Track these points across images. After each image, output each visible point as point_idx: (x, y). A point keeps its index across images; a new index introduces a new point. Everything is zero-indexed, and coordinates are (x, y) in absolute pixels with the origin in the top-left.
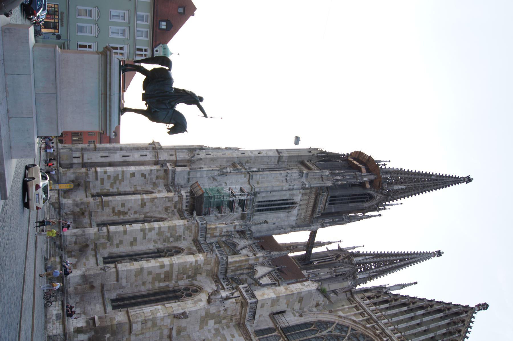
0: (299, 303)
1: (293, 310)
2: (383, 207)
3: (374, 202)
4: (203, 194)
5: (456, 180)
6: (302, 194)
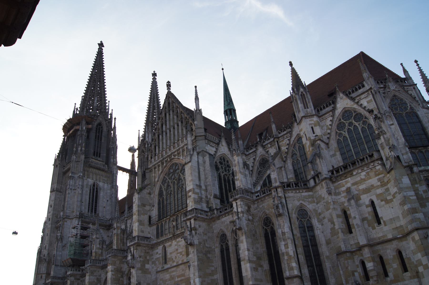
0: (145, 206)
2: (109, 115)
3: (104, 123)
4: (71, 259)
5: (100, 55)
6: (88, 178)
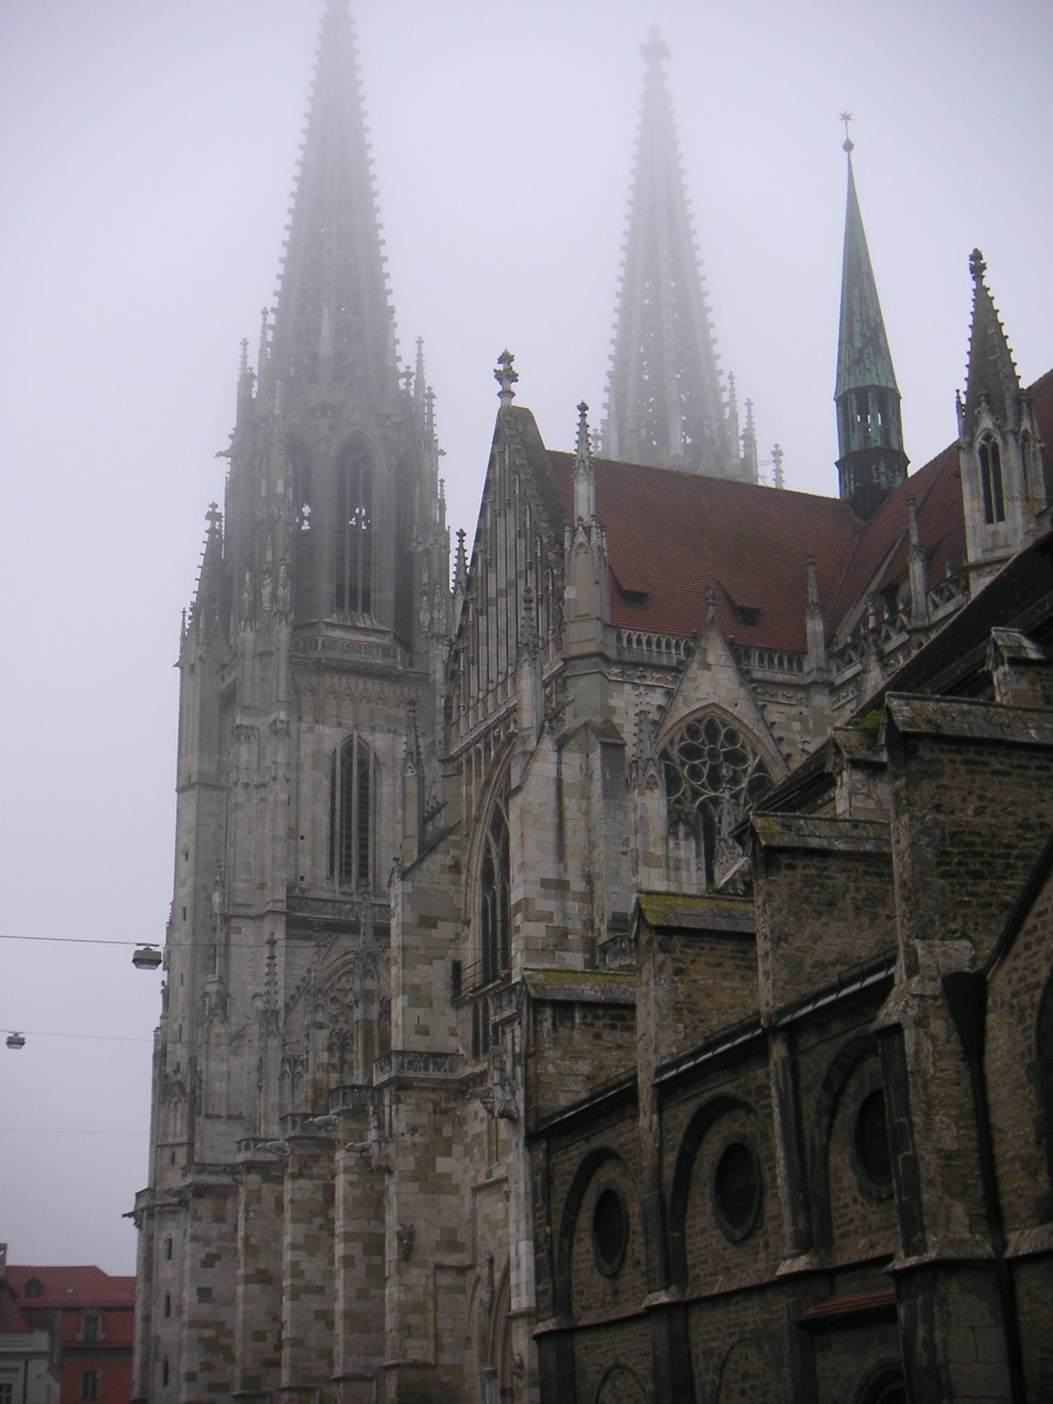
1: (455, 939)
6: (317, 722)
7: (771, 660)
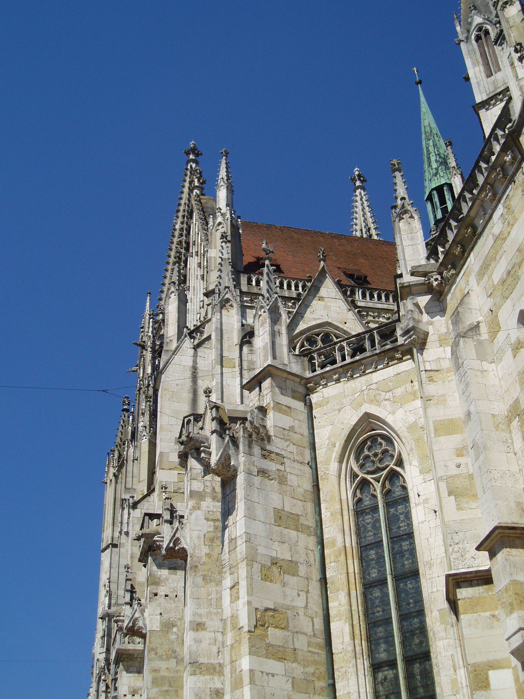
7: (372, 297)
